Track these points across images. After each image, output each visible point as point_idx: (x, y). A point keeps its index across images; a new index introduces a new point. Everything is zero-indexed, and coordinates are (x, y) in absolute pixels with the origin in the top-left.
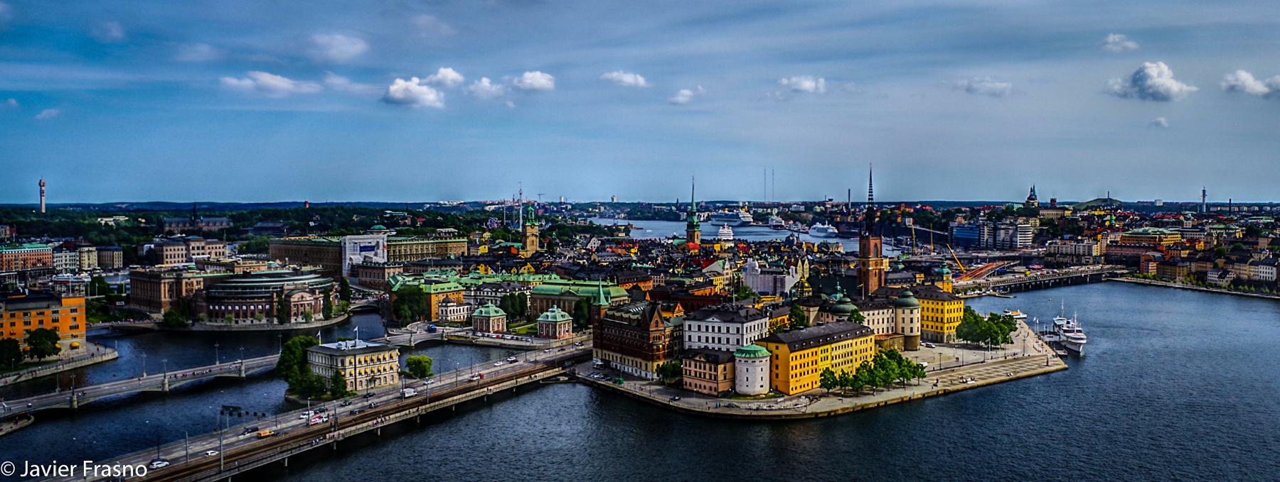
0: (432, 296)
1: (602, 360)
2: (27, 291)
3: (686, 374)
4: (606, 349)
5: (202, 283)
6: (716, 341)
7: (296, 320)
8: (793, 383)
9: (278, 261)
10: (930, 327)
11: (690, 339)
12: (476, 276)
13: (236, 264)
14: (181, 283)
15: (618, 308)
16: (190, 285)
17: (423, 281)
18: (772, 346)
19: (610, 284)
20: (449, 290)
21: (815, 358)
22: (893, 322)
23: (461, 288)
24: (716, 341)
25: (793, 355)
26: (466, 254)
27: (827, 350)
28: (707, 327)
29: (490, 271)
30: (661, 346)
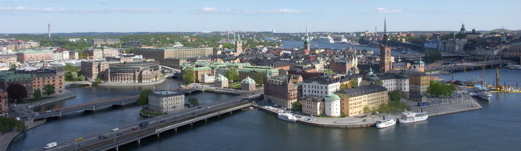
0: (198, 72)
1: (268, 99)
2: (44, 69)
3: (303, 106)
4: (269, 95)
5: (108, 66)
6: (317, 92)
8: (350, 111)
10: (414, 87)
11: (305, 91)
12: (216, 64)
13: (121, 58)
14: (100, 66)
15: (275, 78)
16: (103, 67)
17: (195, 66)
18: (341, 95)
19: (271, 67)
21: (360, 101)
22: (396, 85)
23: (210, 69)
24: (317, 92)
25: (350, 99)
26: (212, 54)
27: (366, 97)
28: (312, 86)
29: (222, 62)
30: (293, 94)
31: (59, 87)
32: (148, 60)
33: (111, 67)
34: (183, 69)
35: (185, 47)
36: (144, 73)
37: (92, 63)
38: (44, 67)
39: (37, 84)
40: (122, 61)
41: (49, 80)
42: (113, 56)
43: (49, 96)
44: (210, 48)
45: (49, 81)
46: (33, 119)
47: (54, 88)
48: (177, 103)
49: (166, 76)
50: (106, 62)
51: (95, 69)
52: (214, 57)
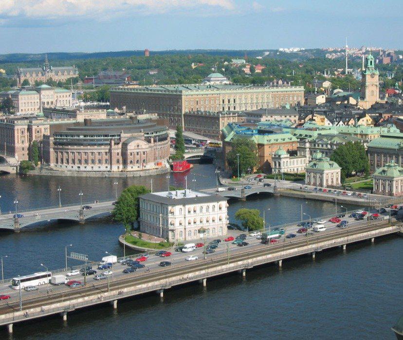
5: (49, 130)
7: (132, 167)
9: (116, 110)
12: (311, 126)
13: (78, 112)
14: (32, 129)
16: (38, 132)
20: (283, 142)
23: (294, 139)
26: (302, 104)
29: (327, 122)
32: (141, 117)
33: (56, 131)
34: (228, 139)
36: (131, 147)
40: (80, 118)
42: (59, 106)
44: (298, 88)
51: (21, 137)
52: (305, 111)
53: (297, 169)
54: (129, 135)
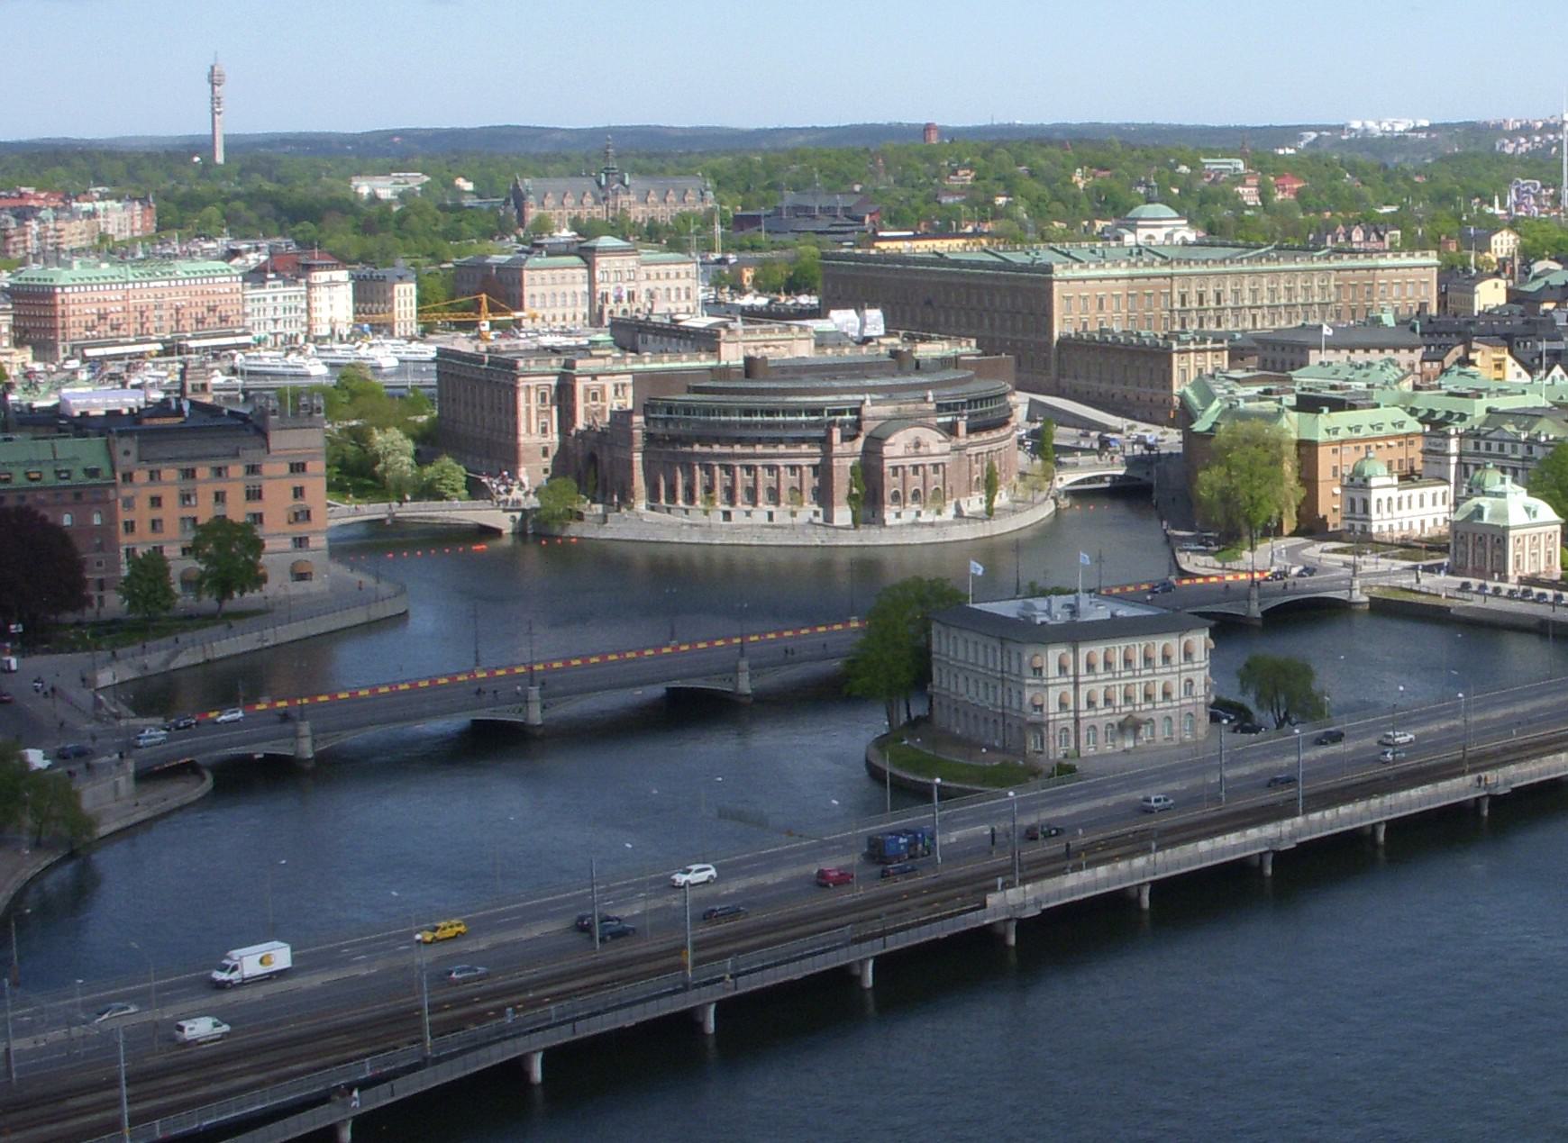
0: (1320, 449)
2: (186, 406)
5: (630, 392)
7: (898, 515)
12: (1464, 385)
13: (723, 332)
14: (573, 388)
16: (595, 397)
17: (1290, 400)
23: (1413, 425)
26: (1433, 310)
29: (1513, 371)
31: (287, 544)
34: (1200, 426)
35: (1212, 245)
36: (896, 448)
37: (512, 365)
38: (189, 390)
39: (142, 514)
40: (732, 354)
41: (220, 486)
43: (228, 605)
44: (1418, 259)
45: (219, 497)
46: (131, 766)
47: (257, 545)
48: (1148, 697)
49: (1066, 479)
50: (610, 359)
51: (539, 412)
53: (1423, 523)
54: (887, 410)
